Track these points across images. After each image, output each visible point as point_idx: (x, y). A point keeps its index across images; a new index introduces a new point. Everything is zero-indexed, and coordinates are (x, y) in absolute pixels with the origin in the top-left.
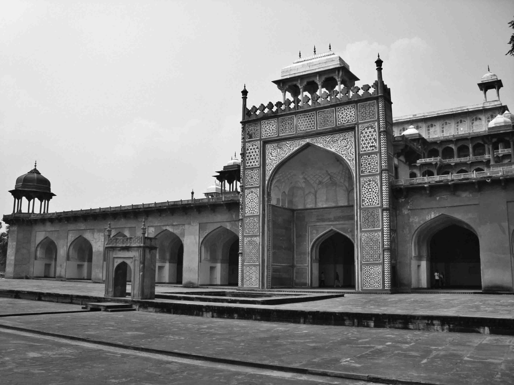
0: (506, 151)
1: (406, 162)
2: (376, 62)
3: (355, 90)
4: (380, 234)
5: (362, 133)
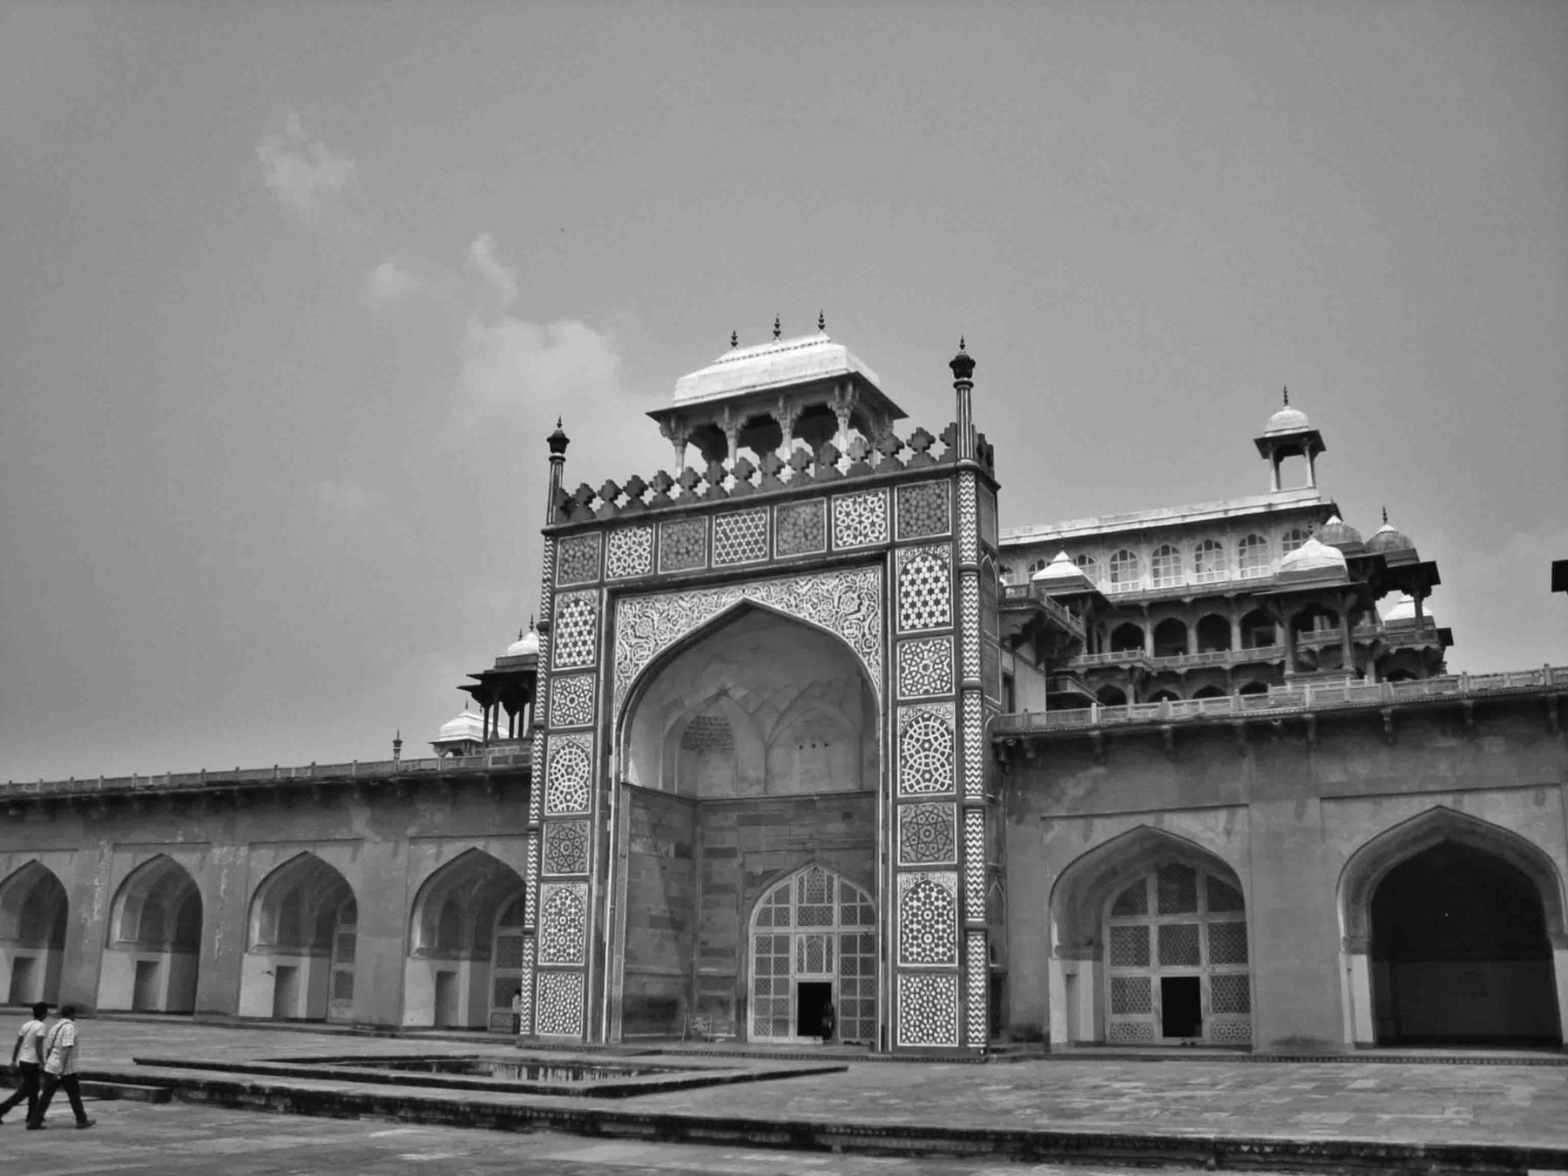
0: (1333, 636)
1: (1038, 662)
2: (952, 365)
3: (889, 445)
4: (954, 876)
5: (906, 572)
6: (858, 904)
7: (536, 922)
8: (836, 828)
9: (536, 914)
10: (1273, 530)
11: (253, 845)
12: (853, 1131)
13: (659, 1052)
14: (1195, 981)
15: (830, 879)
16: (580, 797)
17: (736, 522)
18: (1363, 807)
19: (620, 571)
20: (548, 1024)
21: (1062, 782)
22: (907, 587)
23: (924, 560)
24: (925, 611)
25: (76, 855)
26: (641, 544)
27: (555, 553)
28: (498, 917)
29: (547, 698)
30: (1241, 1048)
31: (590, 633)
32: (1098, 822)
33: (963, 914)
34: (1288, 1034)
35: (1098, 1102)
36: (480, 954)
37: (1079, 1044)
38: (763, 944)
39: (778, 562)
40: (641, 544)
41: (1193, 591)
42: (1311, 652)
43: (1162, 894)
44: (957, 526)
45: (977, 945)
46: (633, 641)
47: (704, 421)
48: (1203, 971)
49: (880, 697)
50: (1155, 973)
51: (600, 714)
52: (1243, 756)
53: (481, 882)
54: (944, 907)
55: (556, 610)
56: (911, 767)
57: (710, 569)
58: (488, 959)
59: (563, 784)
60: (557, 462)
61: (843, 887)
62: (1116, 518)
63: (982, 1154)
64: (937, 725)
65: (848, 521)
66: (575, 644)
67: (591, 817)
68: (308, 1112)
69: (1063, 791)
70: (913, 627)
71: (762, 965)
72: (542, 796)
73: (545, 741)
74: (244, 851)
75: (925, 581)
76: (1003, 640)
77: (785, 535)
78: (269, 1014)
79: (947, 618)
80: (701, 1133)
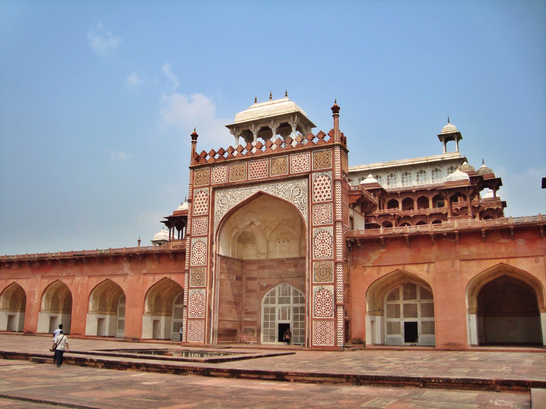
0: (465, 204)
2: (332, 109)
3: (310, 137)
4: (332, 287)
5: (316, 181)
6: (299, 296)
7: (188, 302)
8: (292, 270)
9: (188, 300)
10: (444, 167)
11: (89, 277)
12: (297, 374)
13: (230, 348)
14: (416, 323)
15: (289, 288)
16: (203, 259)
17: (257, 164)
18: (475, 263)
19: (216, 181)
20: (192, 338)
21: (370, 254)
22: (316, 186)
23: (322, 177)
24: (323, 195)
25: (29, 280)
26: (223, 172)
27: (194, 175)
28: (174, 301)
29: (191, 225)
30: (432, 347)
31: (206, 202)
32: (383, 268)
33: (335, 300)
34: (448, 342)
35: (382, 365)
36: (168, 314)
37: (375, 345)
38: (266, 310)
39: (271, 178)
40: (223, 172)
41: (416, 188)
42: (457, 209)
43: (405, 293)
44: (334, 165)
45: (340, 311)
46: (221, 205)
47: (246, 129)
48: (419, 320)
49: (307, 224)
50: (402, 320)
51: (210, 231)
52: (433, 245)
53: (168, 289)
54: (329, 298)
55: (194, 195)
56: (318, 249)
57: (248, 180)
58: (171, 316)
59: (197, 255)
60: (194, 143)
61: (294, 290)
62: (389, 162)
63: (342, 382)
64: (327, 234)
65: (296, 163)
66: (201, 206)
67: (207, 266)
68: (110, 368)
69: (370, 257)
70: (318, 200)
71: (266, 317)
72: (190, 259)
73: (191, 240)
74: (86, 278)
75: (322, 184)
76: (350, 205)
77: (274, 168)
78: (95, 334)
79: (330, 197)
80: (245, 375)
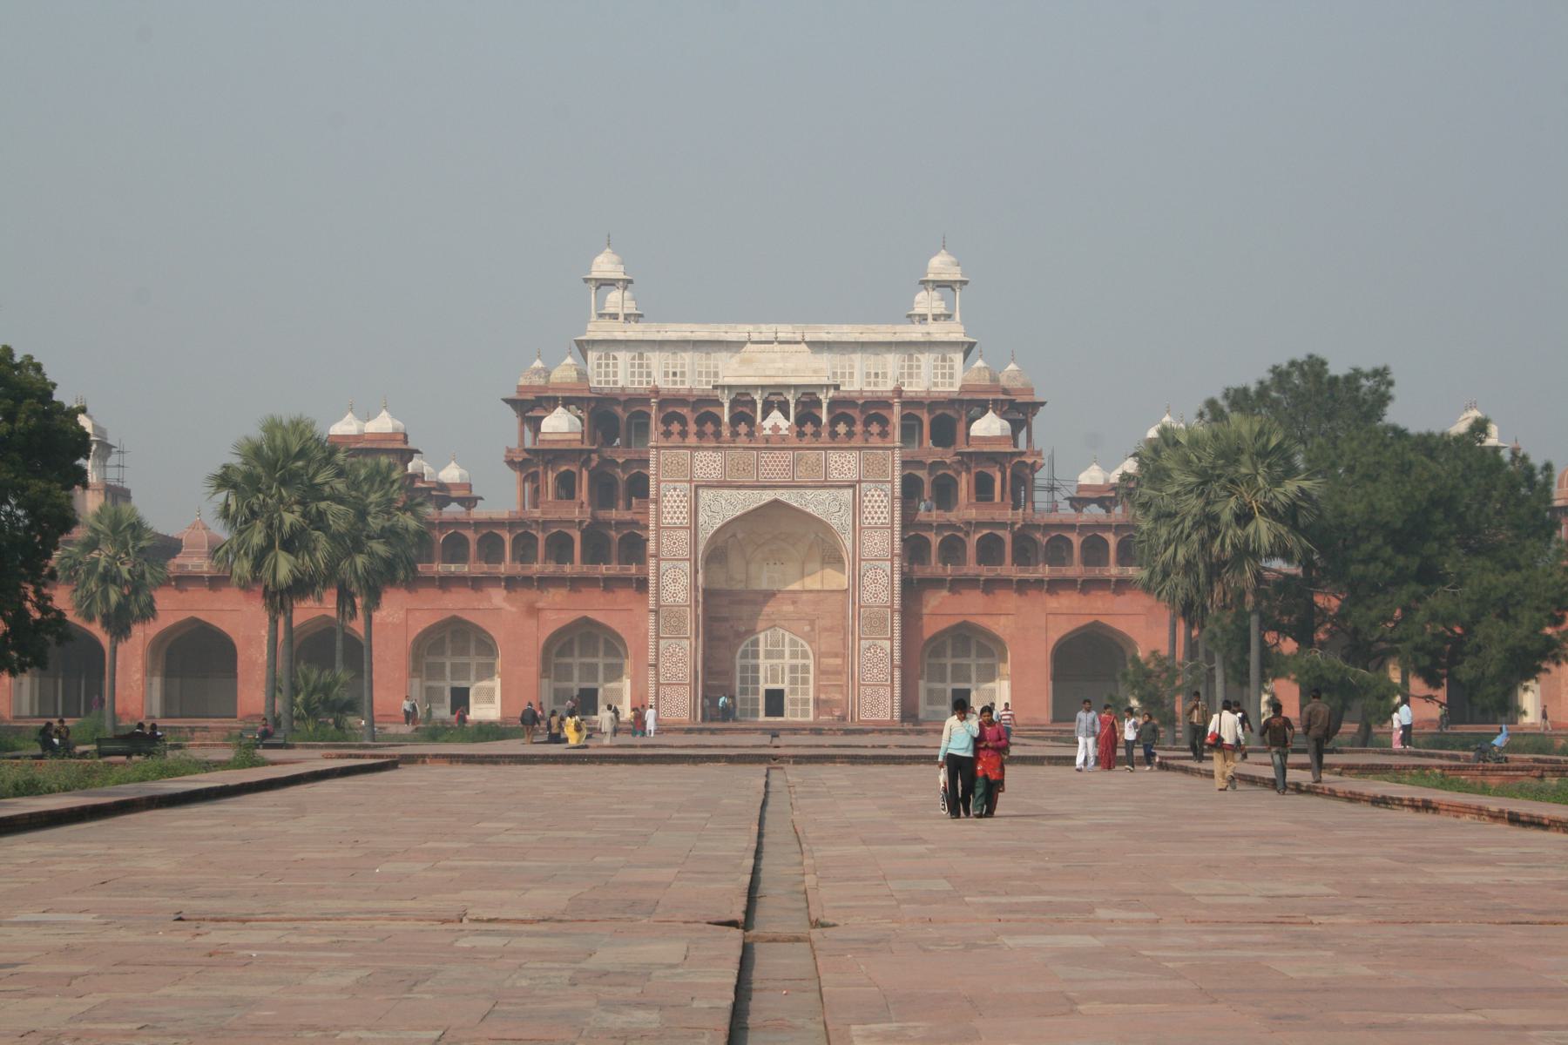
7: (657, 659)
38: (744, 669)
45: (897, 673)
50: (949, 687)
59: (671, 588)
